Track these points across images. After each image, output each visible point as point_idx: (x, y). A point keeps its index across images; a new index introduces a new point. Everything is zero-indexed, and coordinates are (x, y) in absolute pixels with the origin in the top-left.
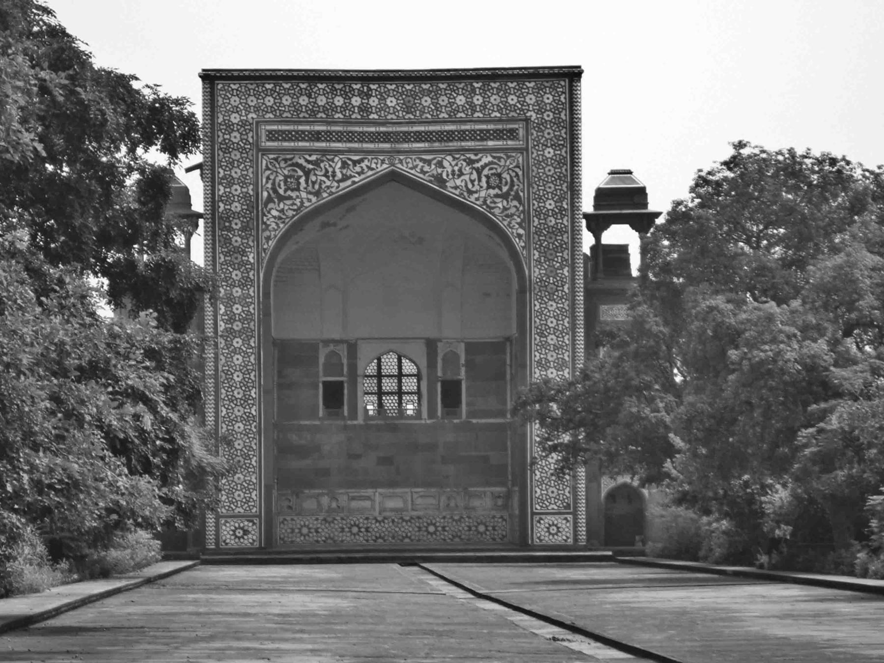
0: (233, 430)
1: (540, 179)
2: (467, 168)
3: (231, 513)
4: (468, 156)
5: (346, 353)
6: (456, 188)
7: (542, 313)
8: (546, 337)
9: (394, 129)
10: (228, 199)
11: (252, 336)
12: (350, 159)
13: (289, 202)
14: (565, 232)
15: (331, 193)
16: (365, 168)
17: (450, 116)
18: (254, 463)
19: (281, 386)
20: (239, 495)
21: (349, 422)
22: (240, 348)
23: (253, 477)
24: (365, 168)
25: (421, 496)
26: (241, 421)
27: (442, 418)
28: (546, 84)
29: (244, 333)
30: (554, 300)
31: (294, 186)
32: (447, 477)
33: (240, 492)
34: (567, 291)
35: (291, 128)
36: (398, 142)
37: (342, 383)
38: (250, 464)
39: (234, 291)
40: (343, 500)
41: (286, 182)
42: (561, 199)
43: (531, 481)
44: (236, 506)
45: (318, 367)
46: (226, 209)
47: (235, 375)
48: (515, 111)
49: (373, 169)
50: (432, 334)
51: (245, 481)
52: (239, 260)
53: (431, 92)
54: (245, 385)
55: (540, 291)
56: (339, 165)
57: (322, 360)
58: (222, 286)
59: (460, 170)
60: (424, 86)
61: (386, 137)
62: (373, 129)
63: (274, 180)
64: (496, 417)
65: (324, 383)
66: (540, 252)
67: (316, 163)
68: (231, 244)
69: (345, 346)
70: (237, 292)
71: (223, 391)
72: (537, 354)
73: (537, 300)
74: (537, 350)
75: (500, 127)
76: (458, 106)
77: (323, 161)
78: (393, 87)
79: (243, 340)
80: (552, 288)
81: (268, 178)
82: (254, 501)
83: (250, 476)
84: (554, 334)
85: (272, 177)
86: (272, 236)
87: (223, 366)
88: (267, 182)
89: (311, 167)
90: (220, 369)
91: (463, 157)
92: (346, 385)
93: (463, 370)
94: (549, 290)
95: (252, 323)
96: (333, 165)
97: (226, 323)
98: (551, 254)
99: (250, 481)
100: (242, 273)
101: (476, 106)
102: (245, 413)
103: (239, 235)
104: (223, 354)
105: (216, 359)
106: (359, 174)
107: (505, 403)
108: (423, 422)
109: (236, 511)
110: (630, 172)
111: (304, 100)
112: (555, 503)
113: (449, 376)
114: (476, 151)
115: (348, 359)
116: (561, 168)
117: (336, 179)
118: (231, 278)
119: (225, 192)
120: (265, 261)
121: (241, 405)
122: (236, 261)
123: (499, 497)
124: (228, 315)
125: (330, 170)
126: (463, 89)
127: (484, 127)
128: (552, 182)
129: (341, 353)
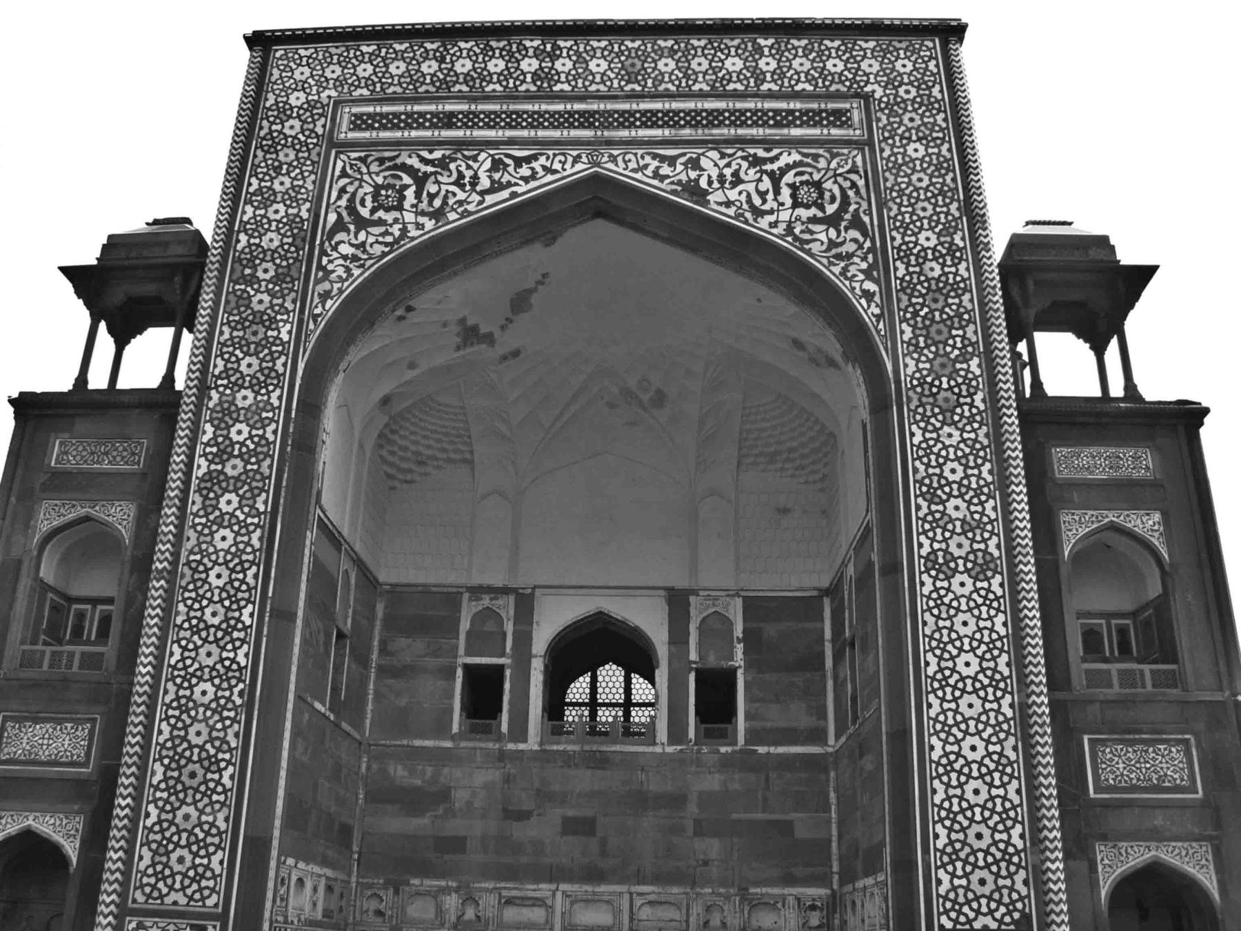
0: (189, 699)
1: (901, 193)
2: (752, 172)
3: (154, 904)
4: (752, 151)
5: (512, 612)
6: (728, 204)
7: (928, 451)
8: (943, 502)
9: (602, 107)
10: (259, 227)
11: (262, 490)
12: (508, 156)
13: (377, 230)
14: (965, 290)
15: (467, 213)
16: (539, 169)
17: (713, 87)
18: (226, 780)
19: (381, 670)
20: (181, 860)
21: (511, 746)
22: (232, 515)
23: (221, 816)
24: (539, 169)
25: (650, 903)
26: (211, 679)
27: (696, 744)
28: (898, 45)
29: (247, 484)
30: (954, 423)
31: (392, 202)
32: (706, 863)
33: (185, 852)
34: (982, 407)
35: (400, 108)
36: (609, 126)
37: (501, 668)
38: (218, 783)
39: (239, 396)
40: (488, 903)
41: (376, 195)
42: (949, 230)
43: (926, 851)
44: (171, 888)
45: (457, 638)
46: (250, 245)
47: (212, 574)
48: (842, 82)
49: (556, 172)
50: (681, 583)
51: (200, 824)
52: (261, 336)
53: (676, 52)
54: (232, 596)
55: (922, 405)
56: (488, 164)
57: (465, 625)
58: (217, 387)
59: (736, 174)
60: (661, 43)
61: (586, 120)
62: (560, 107)
63: (354, 194)
64: (803, 744)
65: (467, 667)
66: (914, 327)
67: (443, 164)
68: (248, 307)
69: (512, 598)
70: (245, 398)
71: (181, 607)
72: (926, 543)
73: (916, 422)
74: (925, 532)
75: (815, 106)
76: (729, 73)
77: (455, 160)
78: (603, 44)
79: (242, 497)
80: (946, 400)
81: (343, 191)
82: (214, 877)
83: (214, 812)
84: (961, 496)
85: (350, 189)
86: (335, 291)
87: (191, 552)
88: (339, 197)
89: (430, 169)
90: (183, 560)
91: (740, 154)
92: (508, 672)
93: (739, 649)
94: (940, 402)
95: (268, 461)
96: (475, 166)
97: (211, 462)
98: (939, 332)
99: (212, 825)
100: (262, 360)
101: (764, 73)
102: (222, 660)
103: (268, 291)
104: (194, 526)
105: (179, 537)
106: (526, 180)
107: (823, 715)
108: (658, 749)
109: (168, 900)
110: (1070, 224)
111: (430, 67)
112: (991, 912)
113: (712, 661)
114: (768, 144)
115: (514, 625)
116: (943, 176)
117: (478, 188)
118: (237, 370)
119: (255, 216)
120: (313, 339)
121: (217, 641)
122: (253, 339)
123: (813, 908)
124: (217, 444)
125: (468, 174)
126: (738, 48)
127: (782, 105)
128: (927, 199)
129: (503, 615)
